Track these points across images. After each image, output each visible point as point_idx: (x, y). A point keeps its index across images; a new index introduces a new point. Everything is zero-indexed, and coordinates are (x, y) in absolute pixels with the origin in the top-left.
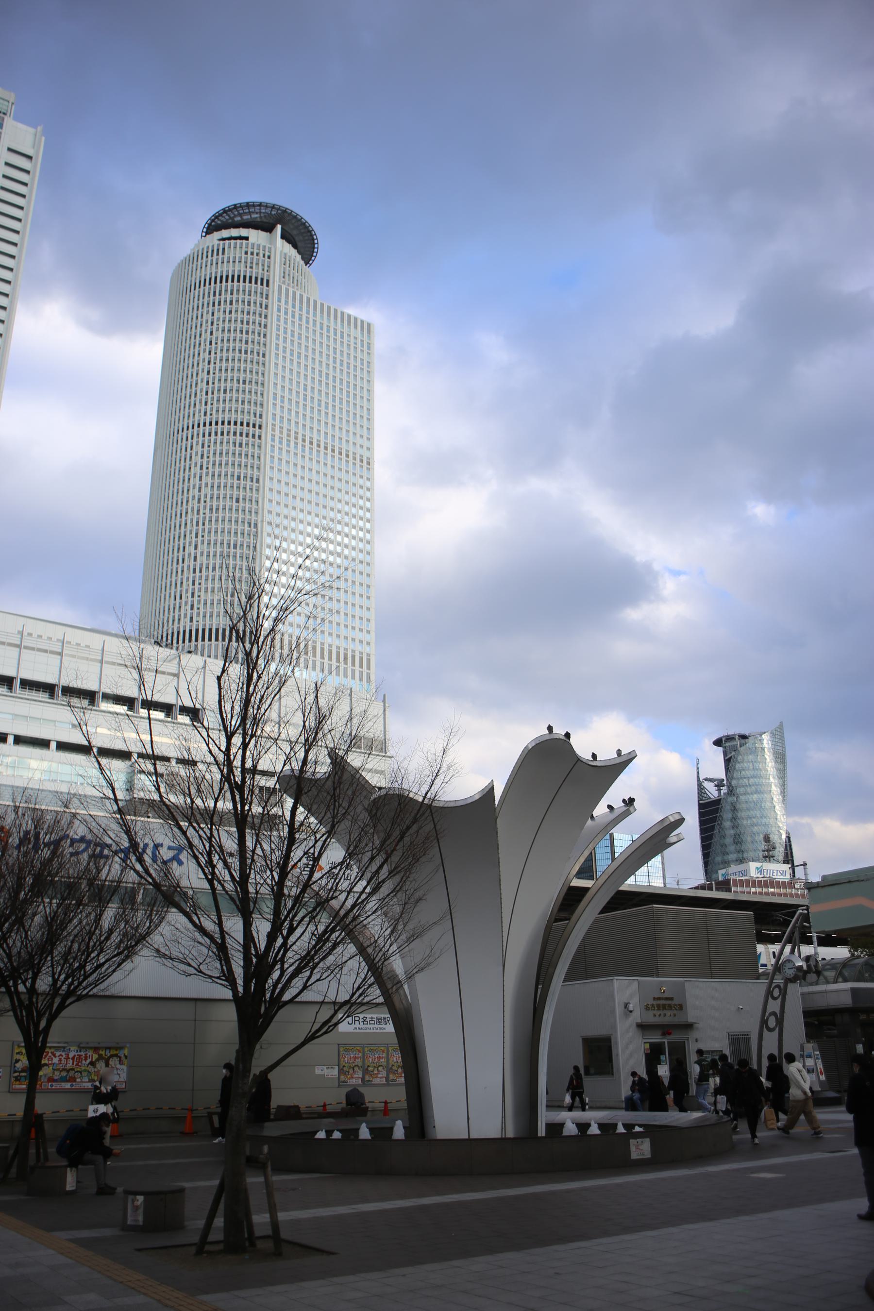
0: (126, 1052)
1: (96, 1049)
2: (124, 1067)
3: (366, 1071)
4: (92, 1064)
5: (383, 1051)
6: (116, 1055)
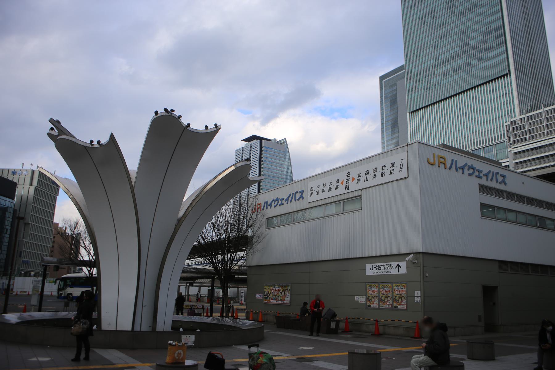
0: (289, 288)
1: (282, 286)
2: (289, 294)
3: (380, 300)
4: (281, 293)
5: (390, 287)
6: (287, 289)
